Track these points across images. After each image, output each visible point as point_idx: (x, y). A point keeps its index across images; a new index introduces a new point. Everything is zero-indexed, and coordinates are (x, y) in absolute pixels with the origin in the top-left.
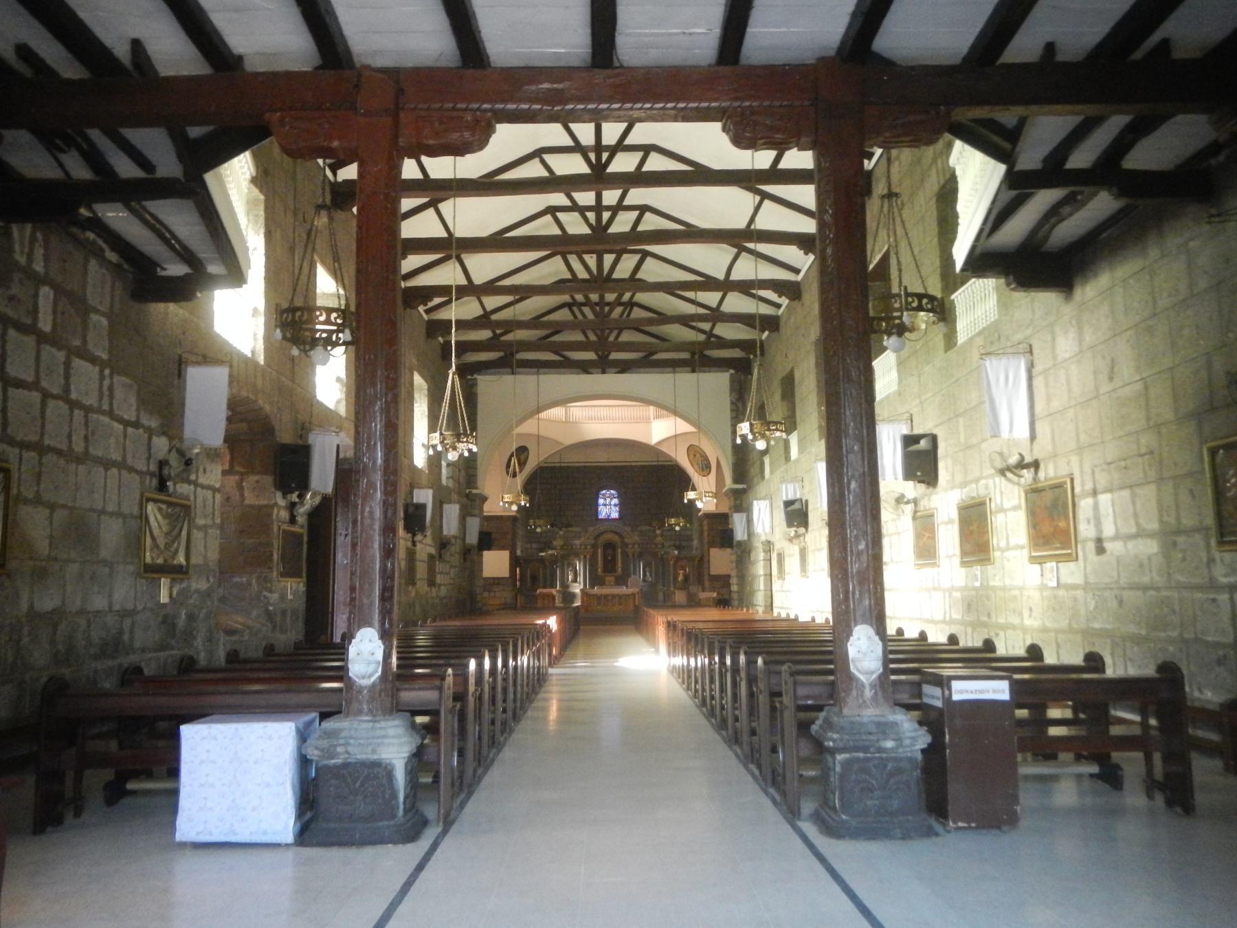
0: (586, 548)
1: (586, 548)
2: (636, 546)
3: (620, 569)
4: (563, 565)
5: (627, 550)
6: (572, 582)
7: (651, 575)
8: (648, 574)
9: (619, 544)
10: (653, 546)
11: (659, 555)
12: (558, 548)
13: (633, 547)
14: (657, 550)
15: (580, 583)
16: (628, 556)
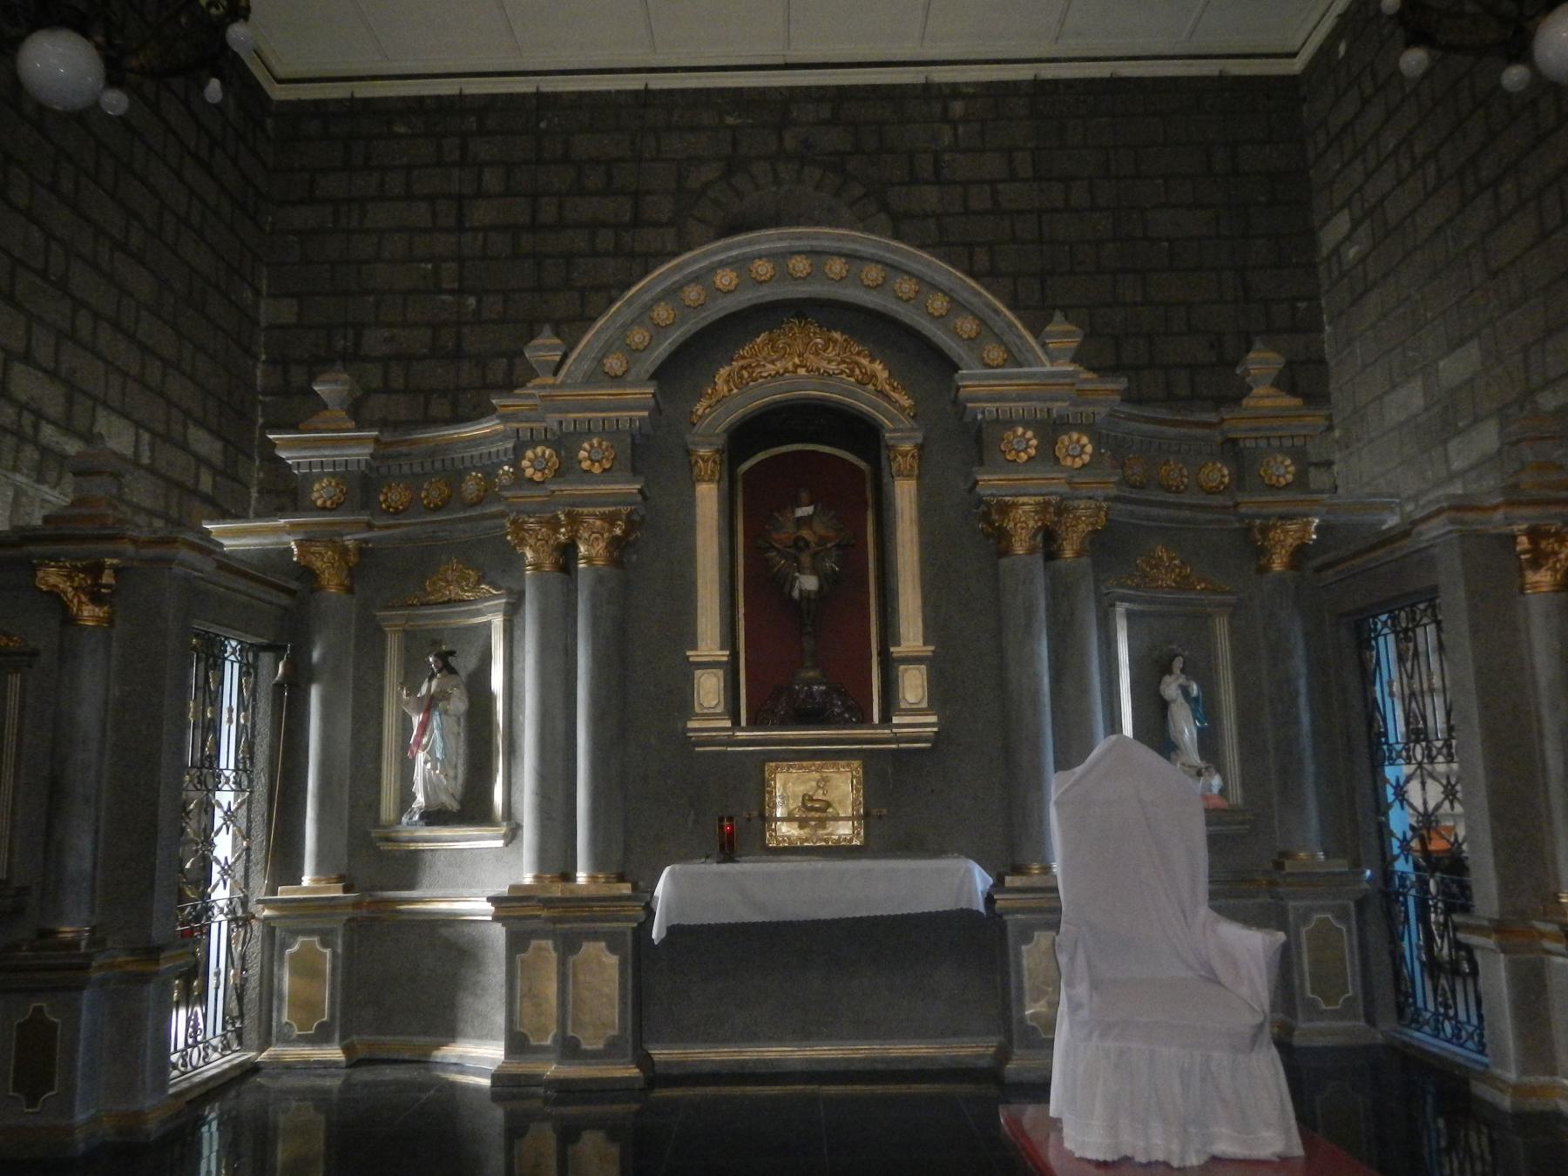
0: (566, 469)
1: (566, 469)
2: (1078, 448)
3: (913, 686)
4: (370, 641)
5: (990, 482)
6: (435, 816)
7: (1209, 744)
8: (1186, 729)
9: (903, 442)
10: (1219, 473)
11: (1286, 538)
12: (320, 492)
13: (1047, 454)
14: (1250, 503)
15: (513, 835)
16: (1000, 541)
